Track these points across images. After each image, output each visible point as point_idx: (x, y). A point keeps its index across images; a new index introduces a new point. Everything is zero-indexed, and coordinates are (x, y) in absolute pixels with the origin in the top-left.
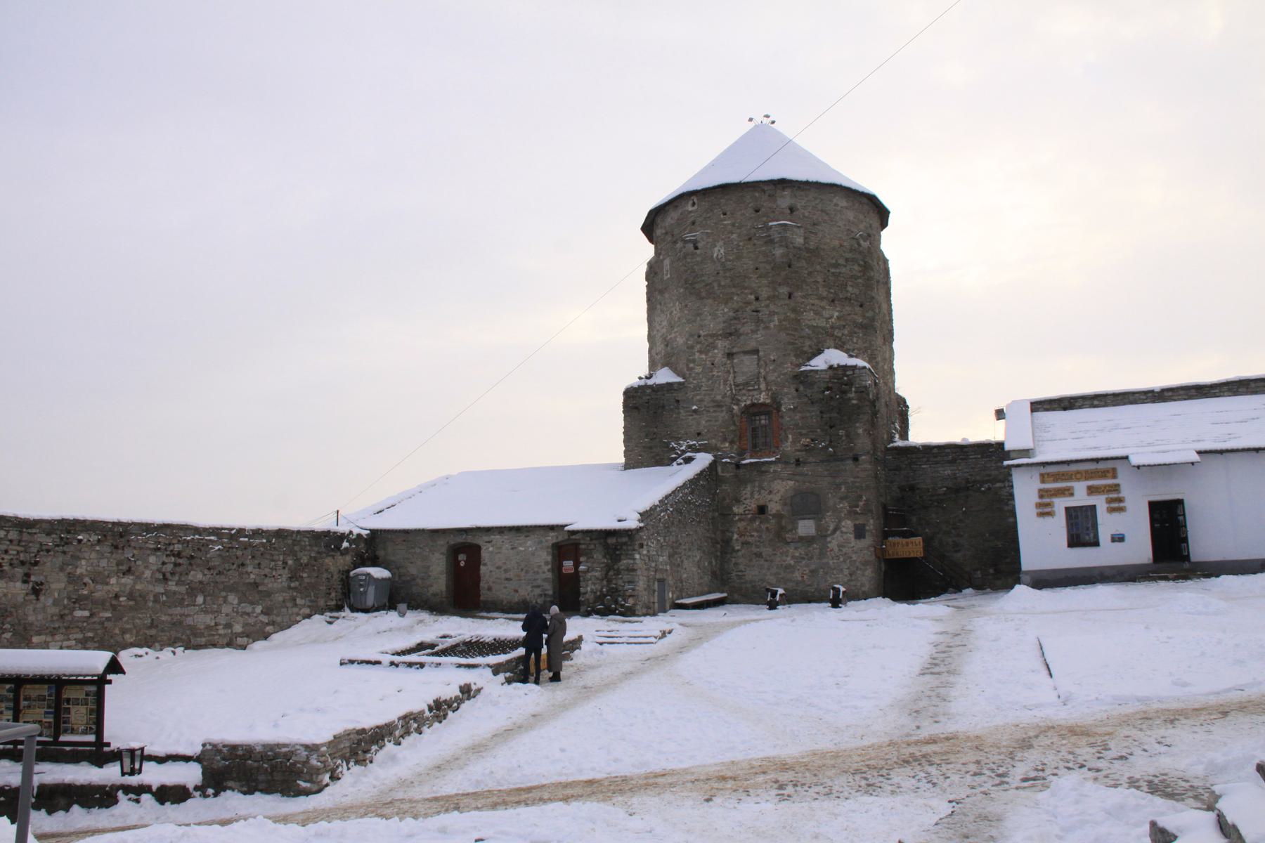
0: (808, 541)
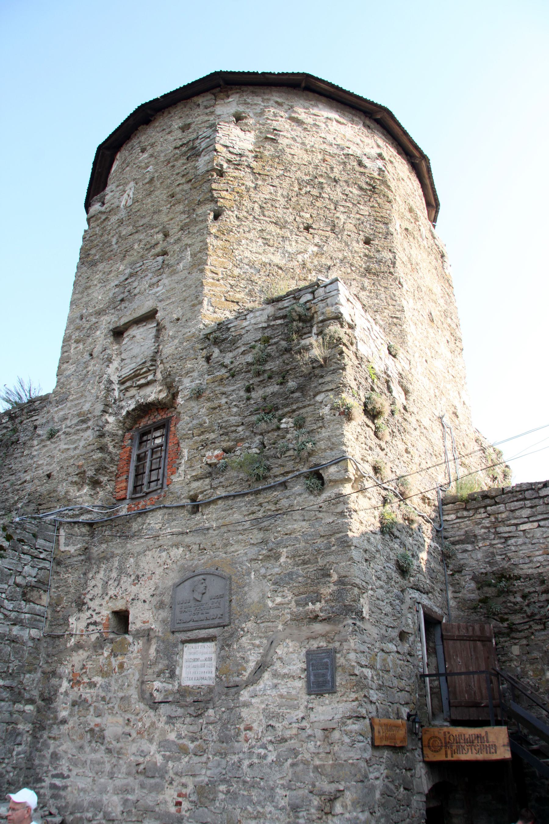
0: (195, 702)
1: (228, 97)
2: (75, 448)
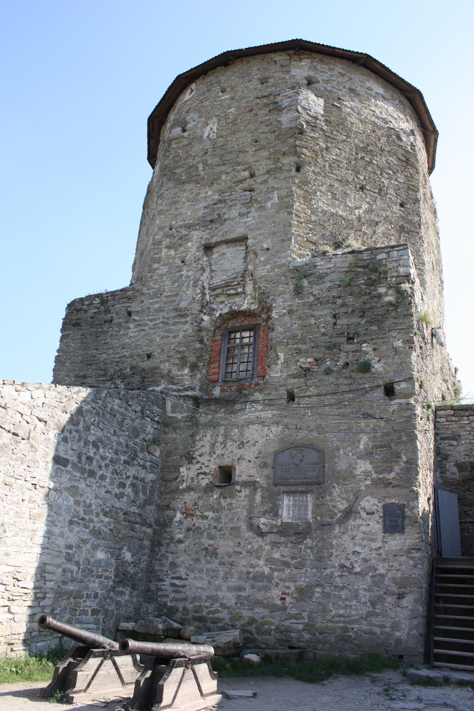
1: (301, 60)
2: (175, 337)
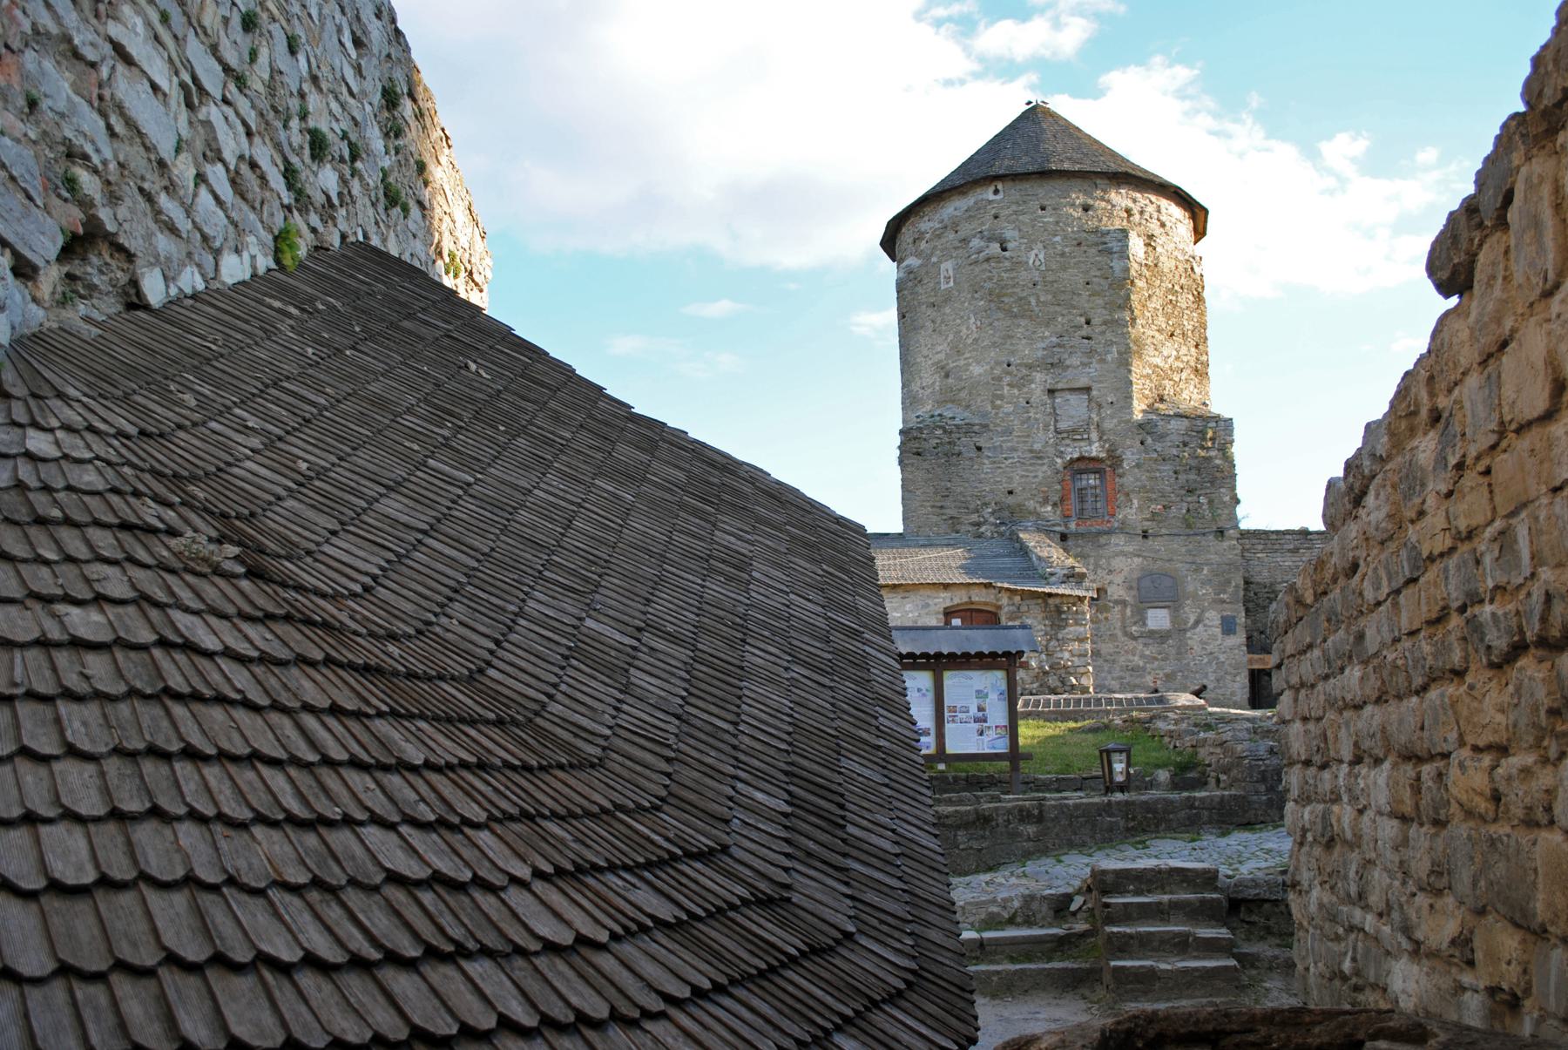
0: (1160, 637)
